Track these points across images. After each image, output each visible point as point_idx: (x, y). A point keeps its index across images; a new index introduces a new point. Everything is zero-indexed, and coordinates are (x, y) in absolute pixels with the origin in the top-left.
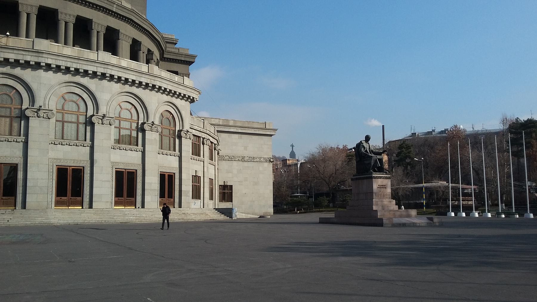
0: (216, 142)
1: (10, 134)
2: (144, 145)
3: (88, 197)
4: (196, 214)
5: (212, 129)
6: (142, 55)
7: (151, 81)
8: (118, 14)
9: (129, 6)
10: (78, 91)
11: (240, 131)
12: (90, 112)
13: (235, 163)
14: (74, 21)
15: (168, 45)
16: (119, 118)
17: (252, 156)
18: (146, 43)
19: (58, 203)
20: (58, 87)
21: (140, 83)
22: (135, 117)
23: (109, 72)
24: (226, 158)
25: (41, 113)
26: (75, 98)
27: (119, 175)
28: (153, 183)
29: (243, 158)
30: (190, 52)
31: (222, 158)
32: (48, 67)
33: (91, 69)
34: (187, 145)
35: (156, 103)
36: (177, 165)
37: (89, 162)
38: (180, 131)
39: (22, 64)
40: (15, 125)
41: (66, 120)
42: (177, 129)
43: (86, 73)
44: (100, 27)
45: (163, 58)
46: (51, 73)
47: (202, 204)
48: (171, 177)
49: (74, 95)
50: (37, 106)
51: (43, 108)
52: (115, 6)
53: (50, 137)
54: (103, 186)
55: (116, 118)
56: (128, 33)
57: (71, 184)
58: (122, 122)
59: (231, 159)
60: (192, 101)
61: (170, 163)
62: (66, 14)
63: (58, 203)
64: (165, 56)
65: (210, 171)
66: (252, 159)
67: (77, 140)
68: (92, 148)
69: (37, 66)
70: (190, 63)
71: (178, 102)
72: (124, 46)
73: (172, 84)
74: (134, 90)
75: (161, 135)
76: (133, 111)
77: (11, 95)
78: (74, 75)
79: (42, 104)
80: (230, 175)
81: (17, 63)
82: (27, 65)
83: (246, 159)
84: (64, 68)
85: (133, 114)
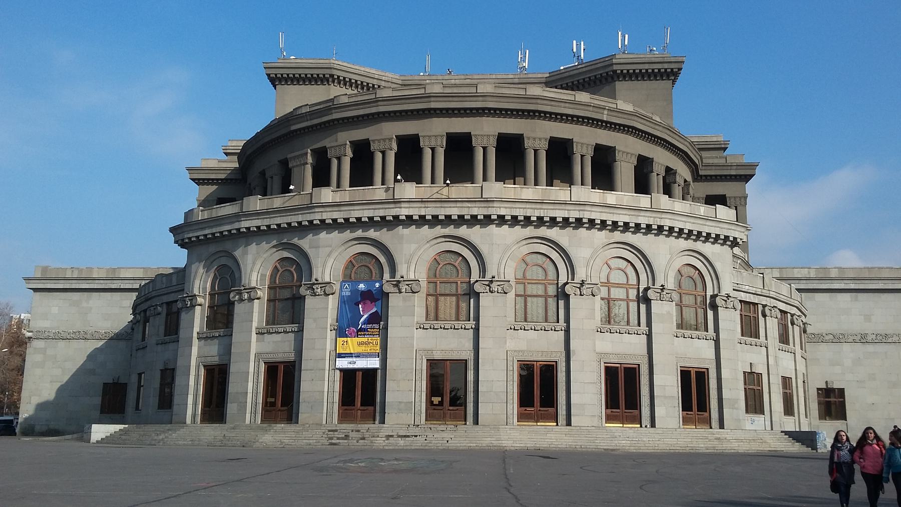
0: (794, 311)
1: (458, 319)
2: (649, 324)
3: (564, 407)
4: (742, 441)
5: (784, 288)
6: (656, 181)
7: (654, 220)
8: (611, 123)
9: (629, 108)
10: (543, 249)
11: (852, 286)
12: (563, 279)
13: (846, 347)
14: (547, 146)
15: (705, 154)
16: (608, 284)
17: (883, 333)
18: (662, 158)
19: (522, 417)
20: (517, 246)
21: (638, 226)
22: (633, 280)
23: (586, 215)
24: (827, 338)
25: (494, 286)
26: (540, 259)
27: (611, 373)
28: (667, 385)
30: (745, 160)
31: (819, 339)
32: (502, 220)
33: (560, 214)
34: (730, 321)
35: (668, 256)
36: (711, 354)
37: (564, 354)
38: (714, 297)
39: (468, 220)
40: (463, 305)
41: (529, 293)
42: (709, 293)
43: (553, 222)
44: (585, 148)
45: (697, 177)
46: (506, 227)
47: (768, 423)
48: (702, 376)
49: (539, 256)
50: (488, 277)
51: (496, 279)
52: (606, 112)
53: (509, 319)
54: (586, 391)
55: (604, 284)
56: (628, 149)
57: (540, 389)
58: (612, 289)
59: (838, 339)
60: (735, 243)
61: (699, 352)
62: (534, 139)
63: (522, 417)
64: (701, 173)
65: (780, 363)
66: (883, 339)
67: (546, 321)
68: (567, 331)
69: (487, 220)
70: (747, 178)
71: (708, 249)
72: (625, 171)
73: (692, 220)
74: (629, 237)
75: (680, 306)
76: (630, 270)
77: (456, 264)
78: (537, 227)
79: (495, 274)
80: (838, 369)
81: (461, 220)
82: (474, 221)
83: (869, 339)
84: (522, 218)
85: (630, 276)
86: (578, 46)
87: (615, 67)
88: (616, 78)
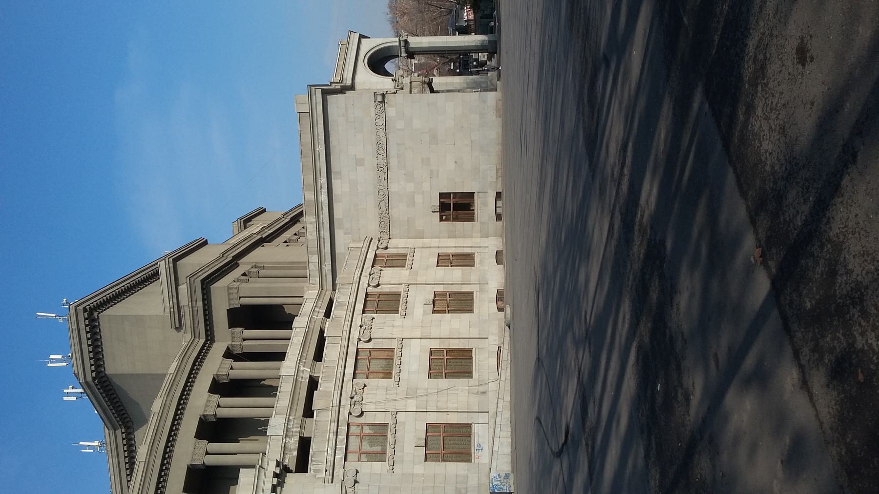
13: (393, 188)
24: (384, 208)
29: (379, 168)
59: (385, 199)
66: (383, 147)
80: (419, 199)
86: (68, 394)
87: (89, 379)
88: (102, 375)
